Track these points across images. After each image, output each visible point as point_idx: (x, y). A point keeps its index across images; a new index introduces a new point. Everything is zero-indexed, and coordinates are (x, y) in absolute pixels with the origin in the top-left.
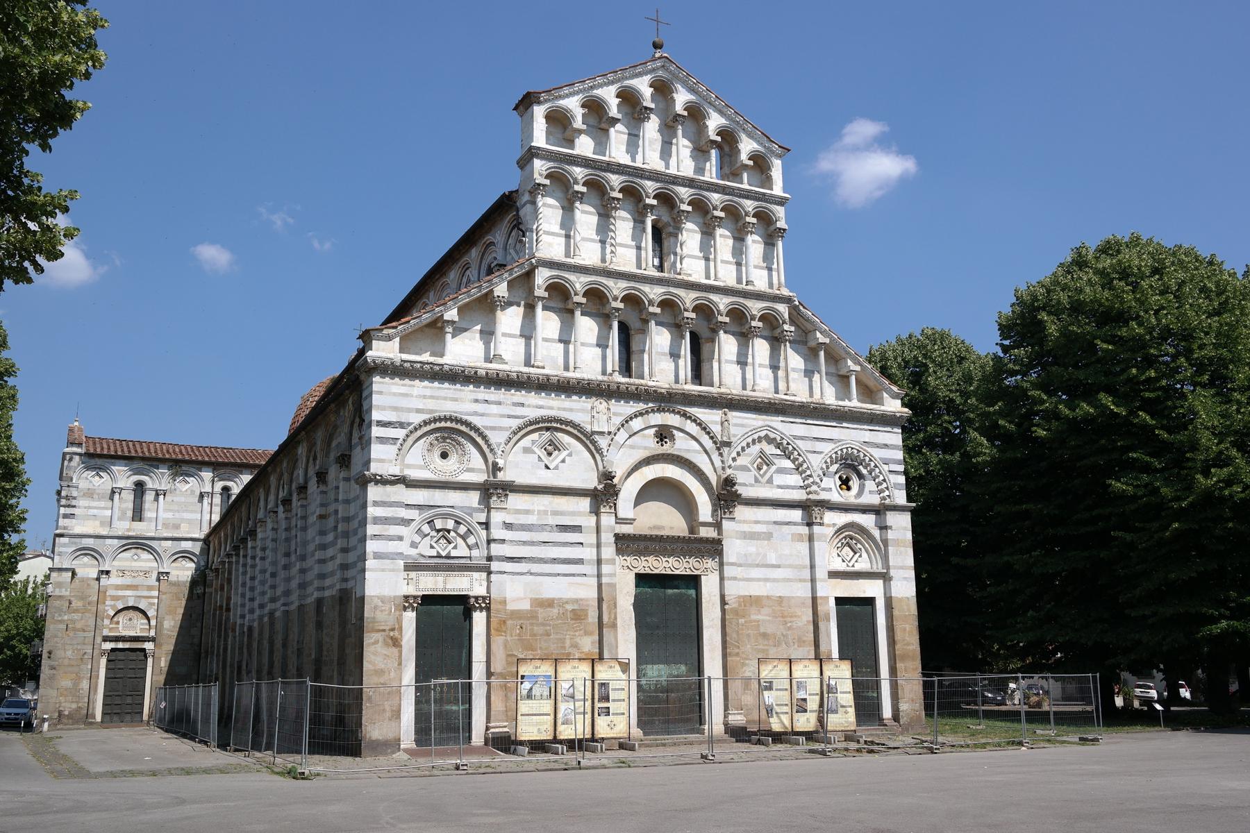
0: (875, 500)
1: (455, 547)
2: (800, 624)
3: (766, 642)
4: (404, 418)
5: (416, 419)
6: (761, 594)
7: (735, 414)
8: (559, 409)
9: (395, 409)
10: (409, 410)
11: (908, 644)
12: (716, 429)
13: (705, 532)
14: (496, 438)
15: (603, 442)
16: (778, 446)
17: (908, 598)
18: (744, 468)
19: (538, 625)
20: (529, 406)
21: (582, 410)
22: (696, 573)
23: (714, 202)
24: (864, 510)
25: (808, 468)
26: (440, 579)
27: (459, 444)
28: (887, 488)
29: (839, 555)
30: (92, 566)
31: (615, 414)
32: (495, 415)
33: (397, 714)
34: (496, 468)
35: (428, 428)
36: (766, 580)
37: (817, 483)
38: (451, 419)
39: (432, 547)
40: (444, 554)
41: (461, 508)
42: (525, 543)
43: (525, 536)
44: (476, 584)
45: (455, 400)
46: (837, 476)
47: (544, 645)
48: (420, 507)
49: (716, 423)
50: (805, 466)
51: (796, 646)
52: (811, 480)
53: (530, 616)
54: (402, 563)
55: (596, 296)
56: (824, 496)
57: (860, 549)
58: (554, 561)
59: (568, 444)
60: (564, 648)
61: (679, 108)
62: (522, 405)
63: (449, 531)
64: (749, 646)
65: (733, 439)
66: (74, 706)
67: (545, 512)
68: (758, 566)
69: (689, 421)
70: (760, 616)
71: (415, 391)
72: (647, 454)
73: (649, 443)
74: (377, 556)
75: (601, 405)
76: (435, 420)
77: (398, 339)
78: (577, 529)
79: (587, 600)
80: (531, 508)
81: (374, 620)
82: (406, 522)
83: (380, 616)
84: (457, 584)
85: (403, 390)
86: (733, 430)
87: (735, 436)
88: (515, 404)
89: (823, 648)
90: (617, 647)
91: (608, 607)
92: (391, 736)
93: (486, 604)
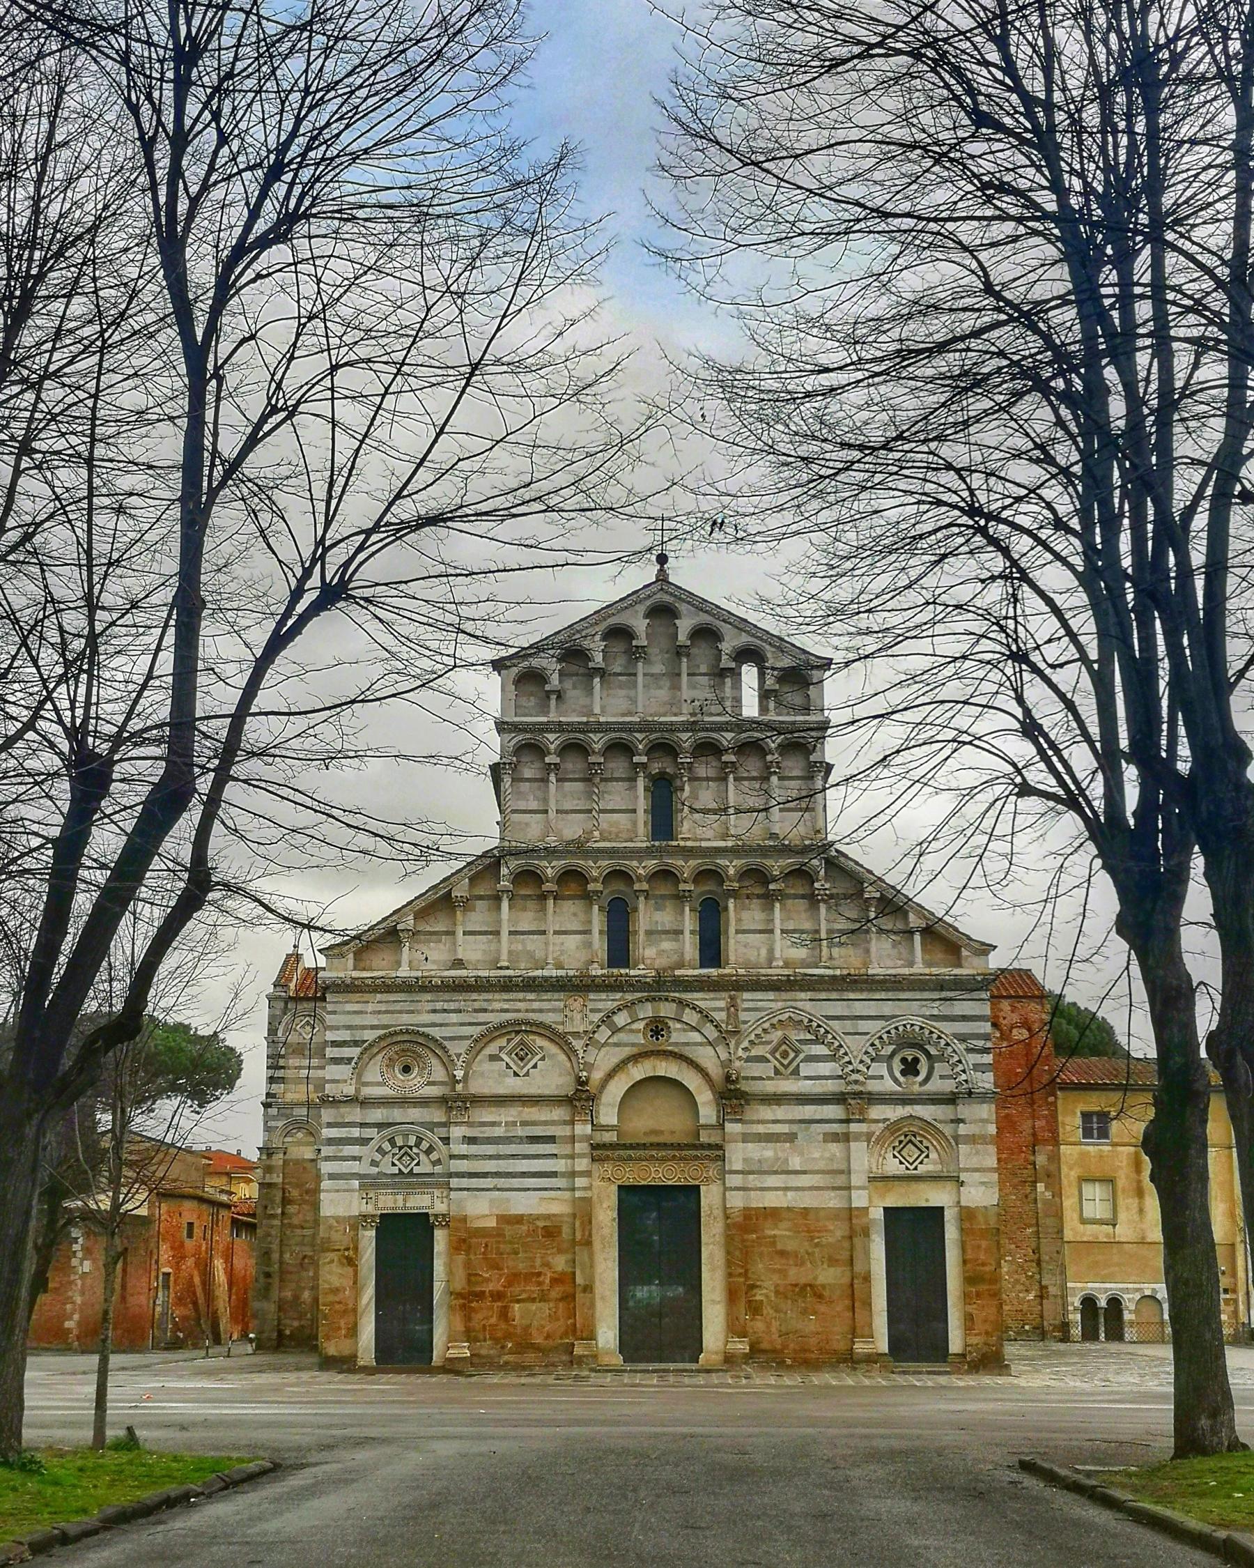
0: (949, 1086)
1: (418, 1164)
2: (830, 1240)
3: (784, 1261)
4: (359, 1035)
5: (370, 1035)
6: (779, 1205)
7: (746, 995)
8: (527, 1011)
9: (349, 1027)
10: (364, 1028)
11: (983, 1264)
12: (720, 1016)
13: (704, 1138)
14: (455, 1048)
15: (578, 1044)
16: (808, 1029)
17: (985, 1207)
18: (762, 1059)
19: (505, 1242)
20: (492, 1011)
21: (553, 1010)
22: (697, 1183)
23: (725, 743)
24: (935, 1099)
25: (846, 1054)
26: (400, 1198)
27: (420, 1056)
28: (964, 1071)
29: (895, 1157)
30: (309, 1144)
31: (592, 1011)
32: (454, 1024)
33: (353, 1332)
34: (454, 1081)
35: (383, 1044)
36: (786, 1189)
37: (858, 1071)
38: (407, 1032)
39: (394, 1165)
40: (406, 1171)
41: (422, 1124)
42: (491, 1157)
43: (490, 1149)
44: (437, 1202)
45: (412, 1012)
46: (897, 1060)
47: (511, 1263)
48: (380, 1126)
49: (721, 1009)
50: (842, 1051)
51: (825, 1266)
52: (851, 1068)
53: (497, 1233)
54: (356, 1183)
55: (572, 876)
56: (873, 1086)
57: (927, 1148)
58: (524, 1175)
59: (541, 1048)
60: (533, 1267)
61: (682, 638)
62: (485, 1011)
63: (411, 1148)
64: (760, 1266)
65: (743, 1027)
66: (296, 1324)
67: (515, 1123)
68: (776, 1173)
69: (687, 1010)
70: (779, 1231)
71: (370, 1007)
72: (635, 1050)
73: (638, 1038)
74: (332, 1177)
75: (577, 1004)
76: (391, 1035)
77: (351, 955)
78: (551, 1139)
79: (561, 1215)
80: (497, 1119)
81: (329, 1240)
82: (364, 1141)
83: (336, 1236)
84: (418, 1202)
85: (357, 1007)
86: (743, 1016)
87: (745, 1022)
88: (476, 1011)
89: (859, 1267)
90: (592, 1266)
91: (582, 1223)
92: (346, 1352)
93: (446, 1220)
